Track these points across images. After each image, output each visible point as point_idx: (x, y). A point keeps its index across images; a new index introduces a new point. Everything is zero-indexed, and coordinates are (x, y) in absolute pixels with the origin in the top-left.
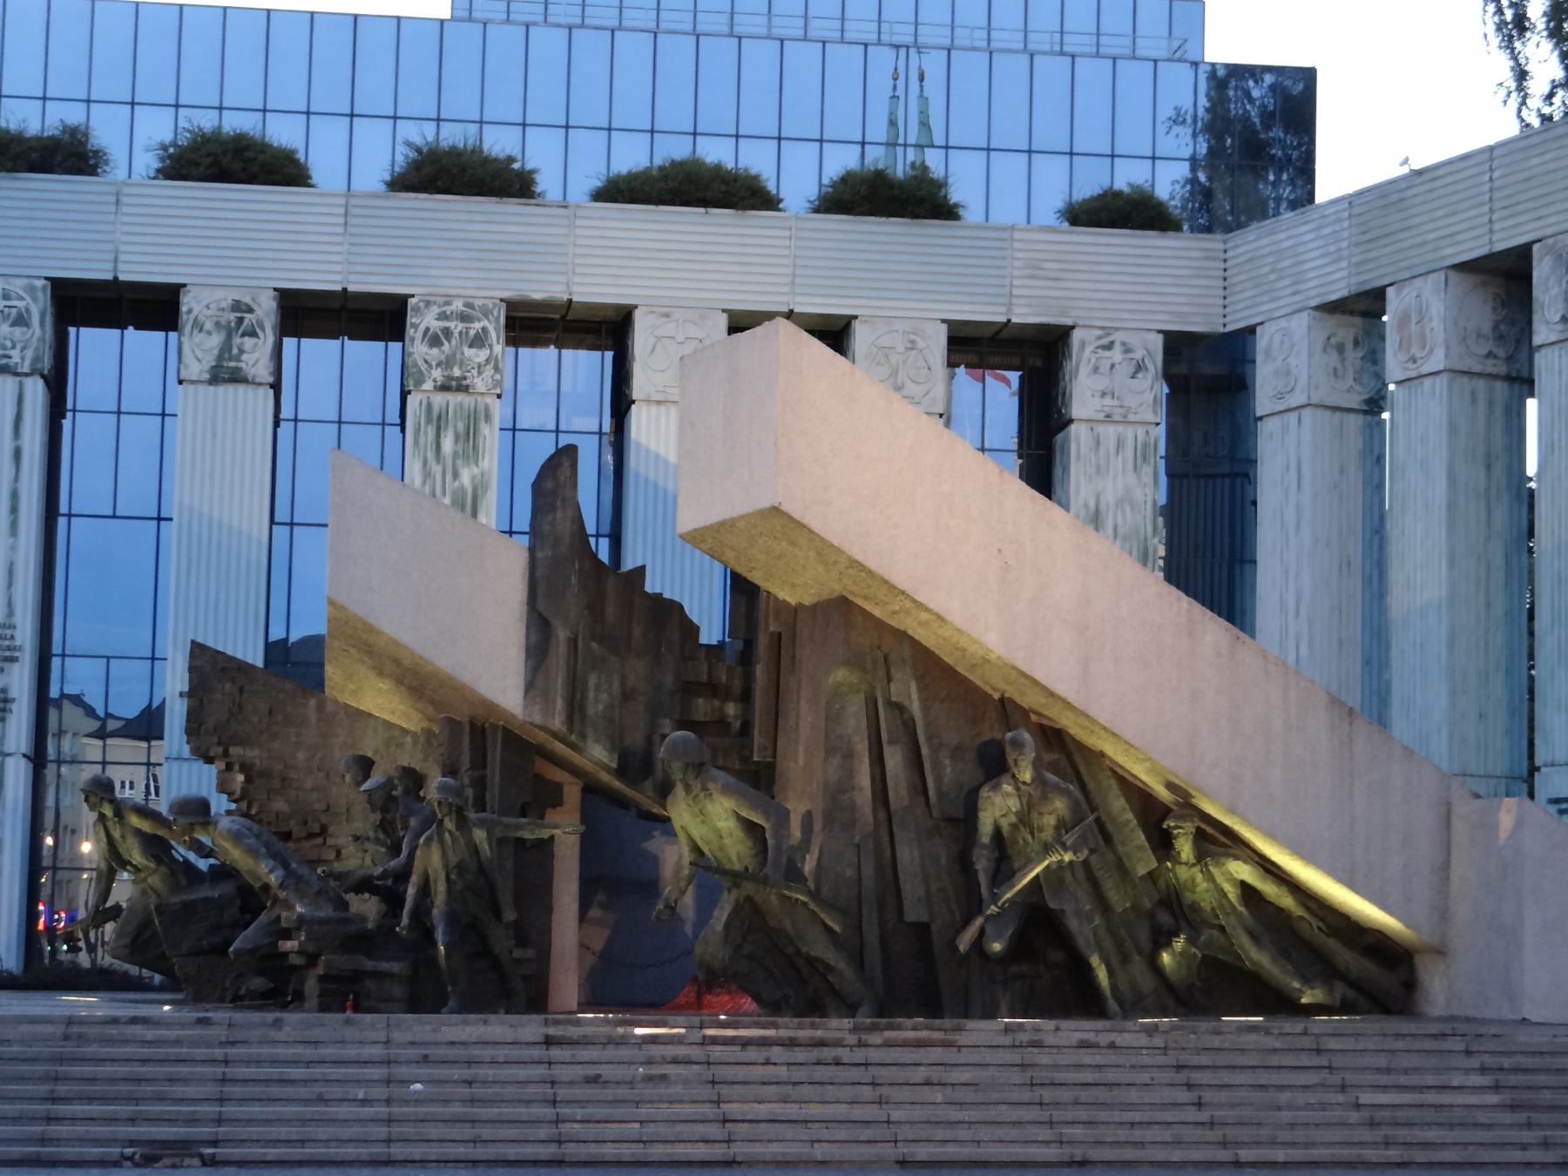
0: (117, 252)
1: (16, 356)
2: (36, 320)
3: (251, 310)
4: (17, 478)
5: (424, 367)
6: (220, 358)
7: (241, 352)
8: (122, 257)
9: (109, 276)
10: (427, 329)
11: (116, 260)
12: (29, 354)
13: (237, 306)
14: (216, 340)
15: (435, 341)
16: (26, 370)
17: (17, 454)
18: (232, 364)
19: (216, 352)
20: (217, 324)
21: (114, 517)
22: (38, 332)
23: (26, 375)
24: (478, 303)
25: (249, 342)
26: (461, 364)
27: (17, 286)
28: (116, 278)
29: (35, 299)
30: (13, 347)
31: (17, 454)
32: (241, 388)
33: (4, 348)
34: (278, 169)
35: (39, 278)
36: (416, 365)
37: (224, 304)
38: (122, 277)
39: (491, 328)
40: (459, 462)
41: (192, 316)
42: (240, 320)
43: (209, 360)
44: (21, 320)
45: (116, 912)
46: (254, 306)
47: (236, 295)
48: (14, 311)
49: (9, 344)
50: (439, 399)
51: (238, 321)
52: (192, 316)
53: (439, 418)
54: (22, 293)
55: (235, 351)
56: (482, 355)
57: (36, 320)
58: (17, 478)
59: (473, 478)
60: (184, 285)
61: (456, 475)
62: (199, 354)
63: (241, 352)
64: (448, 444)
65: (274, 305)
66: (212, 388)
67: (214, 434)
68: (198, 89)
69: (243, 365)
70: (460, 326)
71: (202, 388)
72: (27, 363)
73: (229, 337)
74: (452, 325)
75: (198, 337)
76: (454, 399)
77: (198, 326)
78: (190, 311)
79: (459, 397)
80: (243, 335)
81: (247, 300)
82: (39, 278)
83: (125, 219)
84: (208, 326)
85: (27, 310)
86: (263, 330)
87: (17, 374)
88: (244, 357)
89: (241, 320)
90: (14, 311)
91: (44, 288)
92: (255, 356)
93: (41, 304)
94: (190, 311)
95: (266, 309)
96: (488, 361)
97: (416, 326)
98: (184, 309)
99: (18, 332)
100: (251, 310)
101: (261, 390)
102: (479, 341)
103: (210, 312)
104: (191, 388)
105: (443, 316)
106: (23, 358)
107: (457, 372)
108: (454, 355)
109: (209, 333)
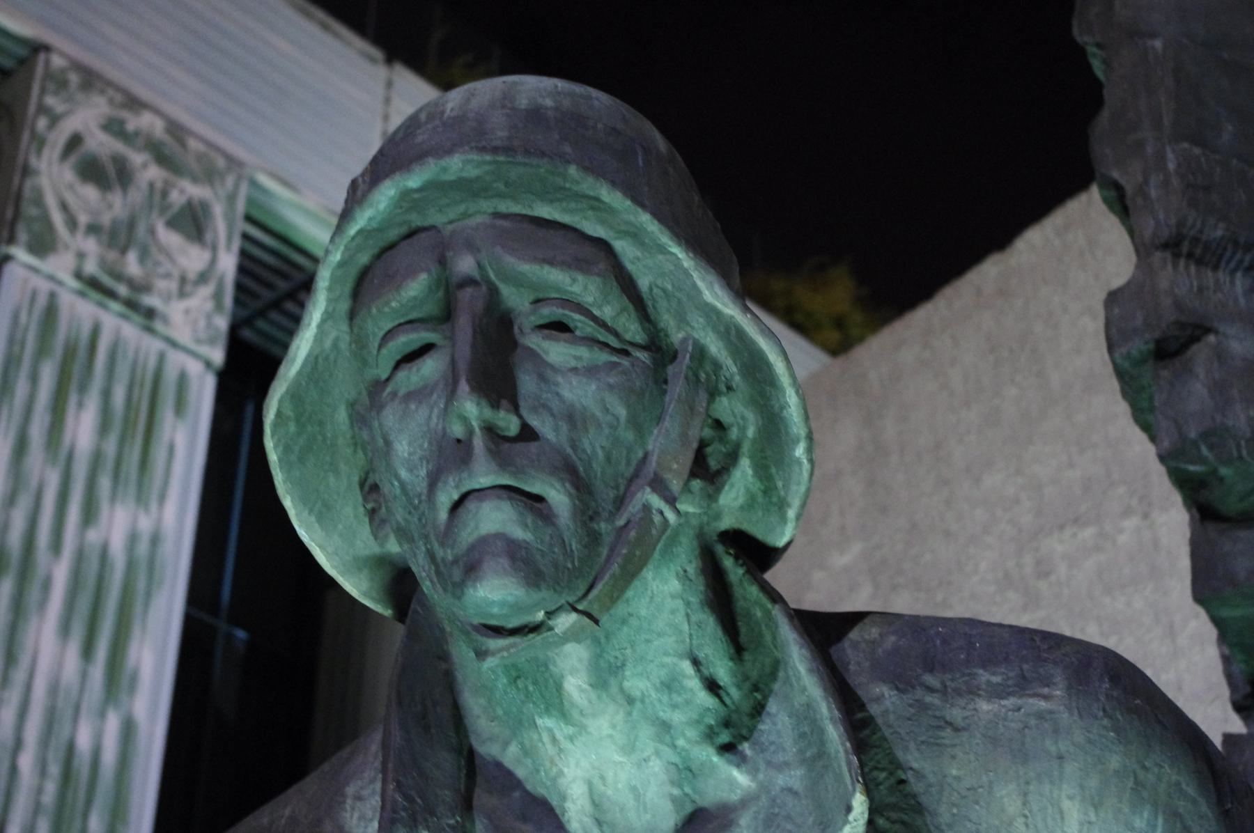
5: (57, 218)
10: (75, 141)
15: (92, 171)
24: (193, 144)
26: (144, 255)
36: (39, 201)
39: (218, 210)
40: (105, 483)
50: (81, 311)
53: (70, 353)
56: (193, 259)
59: (133, 538)
61: (89, 514)
64: (83, 428)
70: (154, 173)
74: (137, 158)
76: (114, 323)
79: (130, 331)
96: (203, 278)
97: (55, 120)
102: (193, 222)
105: (114, 127)
107: (132, 265)
108: (131, 224)
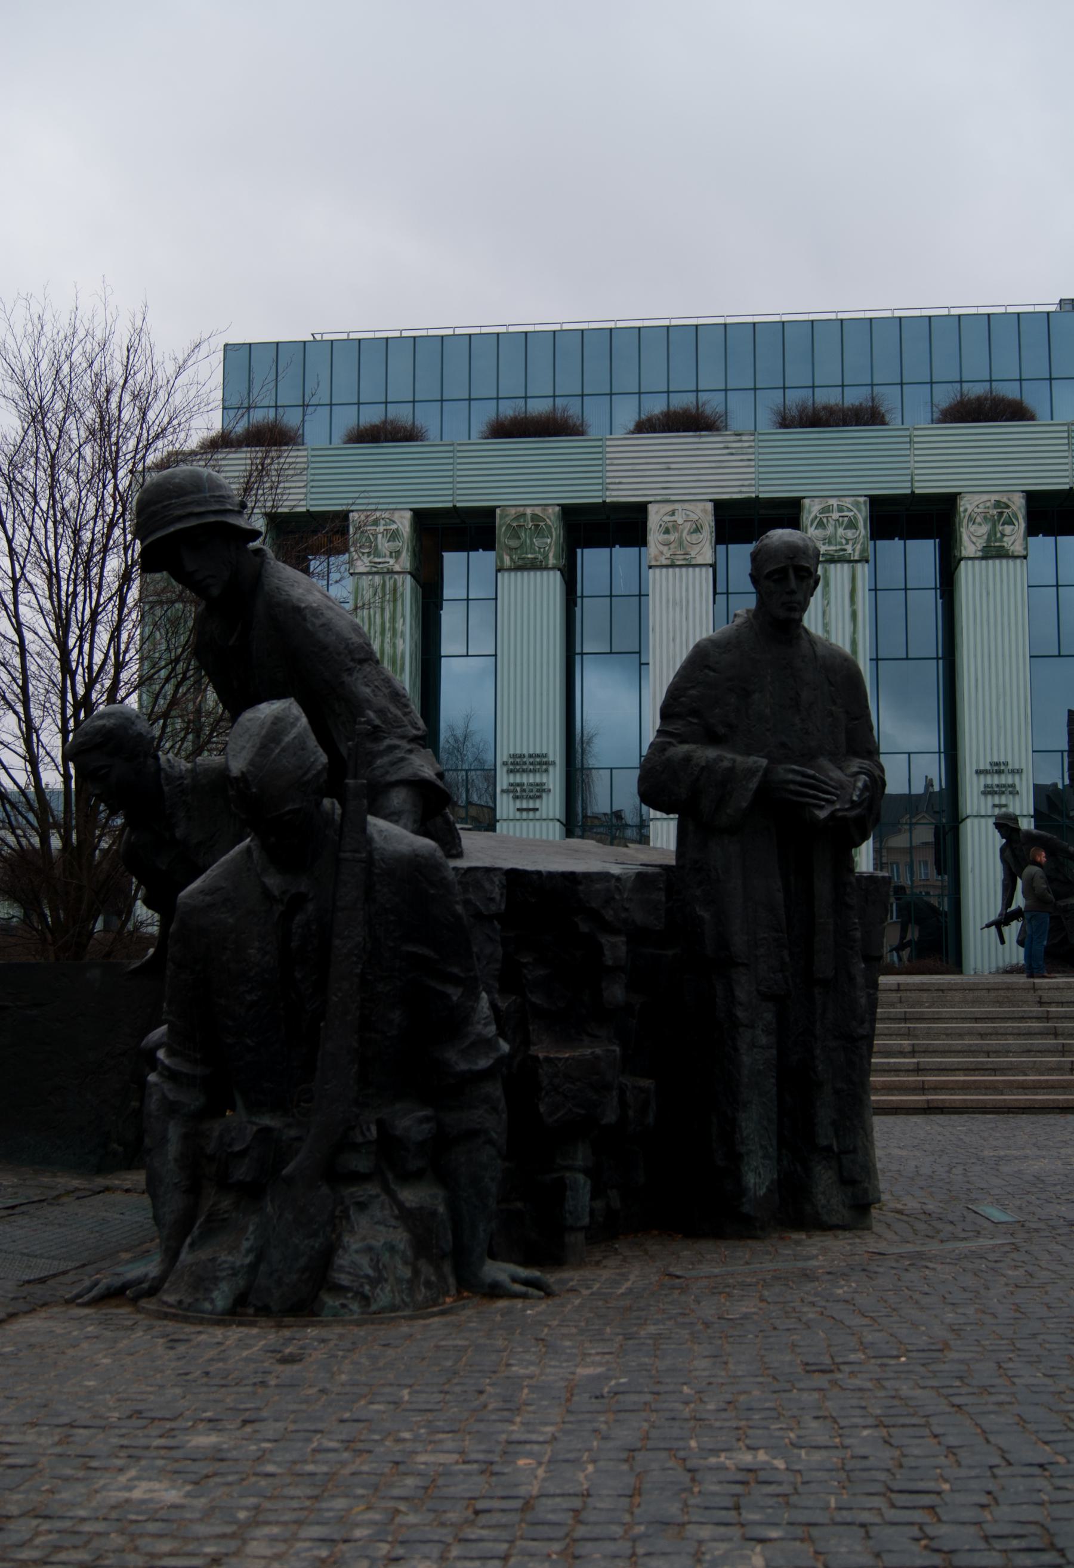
0: (912, 475)
1: (849, 548)
2: (861, 524)
3: (1008, 507)
4: (855, 631)
6: (988, 540)
7: (1003, 535)
8: (916, 478)
9: (908, 491)
11: (912, 481)
12: (858, 547)
13: (998, 504)
14: (984, 529)
16: (856, 558)
17: (854, 615)
18: (997, 544)
19: (985, 537)
20: (985, 518)
21: (907, 659)
22: (863, 532)
23: (857, 561)
25: (1008, 529)
27: (847, 502)
28: (913, 492)
29: (859, 511)
30: (847, 544)
31: (854, 615)
32: (1004, 561)
33: (841, 544)
34: (1014, 412)
35: (860, 496)
37: (988, 504)
38: (917, 491)
41: (967, 514)
42: (1001, 514)
43: (981, 543)
44: (852, 525)
45: (1017, 914)
46: (1010, 504)
47: (996, 497)
48: (846, 519)
49: (844, 541)
51: (1000, 514)
52: (967, 514)
54: (850, 506)
55: (999, 535)
57: (861, 524)
58: (855, 631)
60: (960, 493)
62: (974, 539)
63: (1003, 535)
65: (1023, 501)
66: (984, 562)
67: (988, 594)
68: (945, 370)
69: (1005, 544)
71: (977, 562)
72: (857, 553)
73: (994, 526)
75: (972, 528)
77: (972, 520)
78: (966, 510)
80: (1003, 524)
81: (1005, 500)
82: (860, 496)
83: (916, 452)
84: (979, 520)
85: (855, 518)
86: (1018, 520)
87: (849, 561)
88: (1005, 539)
89: (1001, 514)
90: (846, 519)
91: (865, 502)
92: (1013, 538)
93: (864, 514)
94: (966, 510)
95: (1018, 503)
98: (962, 509)
99: (850, 534)
100: (1008, 507)
101: (1018, 561)
103: (979, 510)
104: (970, 562)
106: (854, 550)
109: (980, 524)
